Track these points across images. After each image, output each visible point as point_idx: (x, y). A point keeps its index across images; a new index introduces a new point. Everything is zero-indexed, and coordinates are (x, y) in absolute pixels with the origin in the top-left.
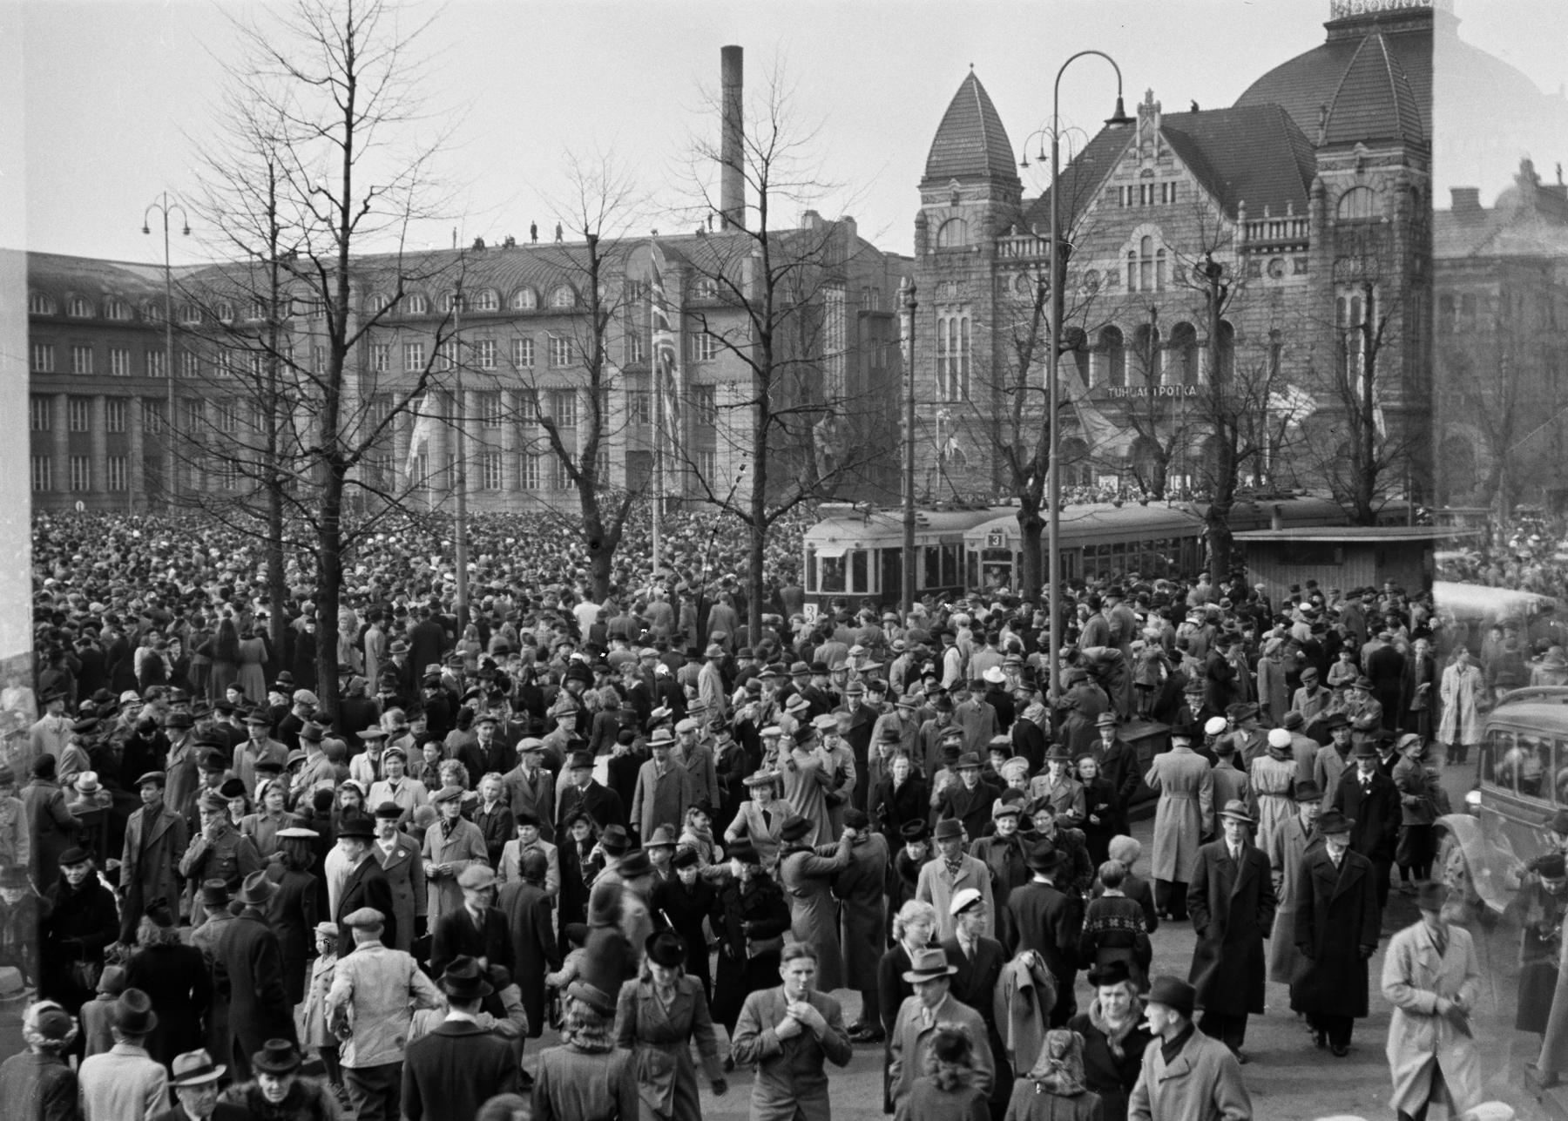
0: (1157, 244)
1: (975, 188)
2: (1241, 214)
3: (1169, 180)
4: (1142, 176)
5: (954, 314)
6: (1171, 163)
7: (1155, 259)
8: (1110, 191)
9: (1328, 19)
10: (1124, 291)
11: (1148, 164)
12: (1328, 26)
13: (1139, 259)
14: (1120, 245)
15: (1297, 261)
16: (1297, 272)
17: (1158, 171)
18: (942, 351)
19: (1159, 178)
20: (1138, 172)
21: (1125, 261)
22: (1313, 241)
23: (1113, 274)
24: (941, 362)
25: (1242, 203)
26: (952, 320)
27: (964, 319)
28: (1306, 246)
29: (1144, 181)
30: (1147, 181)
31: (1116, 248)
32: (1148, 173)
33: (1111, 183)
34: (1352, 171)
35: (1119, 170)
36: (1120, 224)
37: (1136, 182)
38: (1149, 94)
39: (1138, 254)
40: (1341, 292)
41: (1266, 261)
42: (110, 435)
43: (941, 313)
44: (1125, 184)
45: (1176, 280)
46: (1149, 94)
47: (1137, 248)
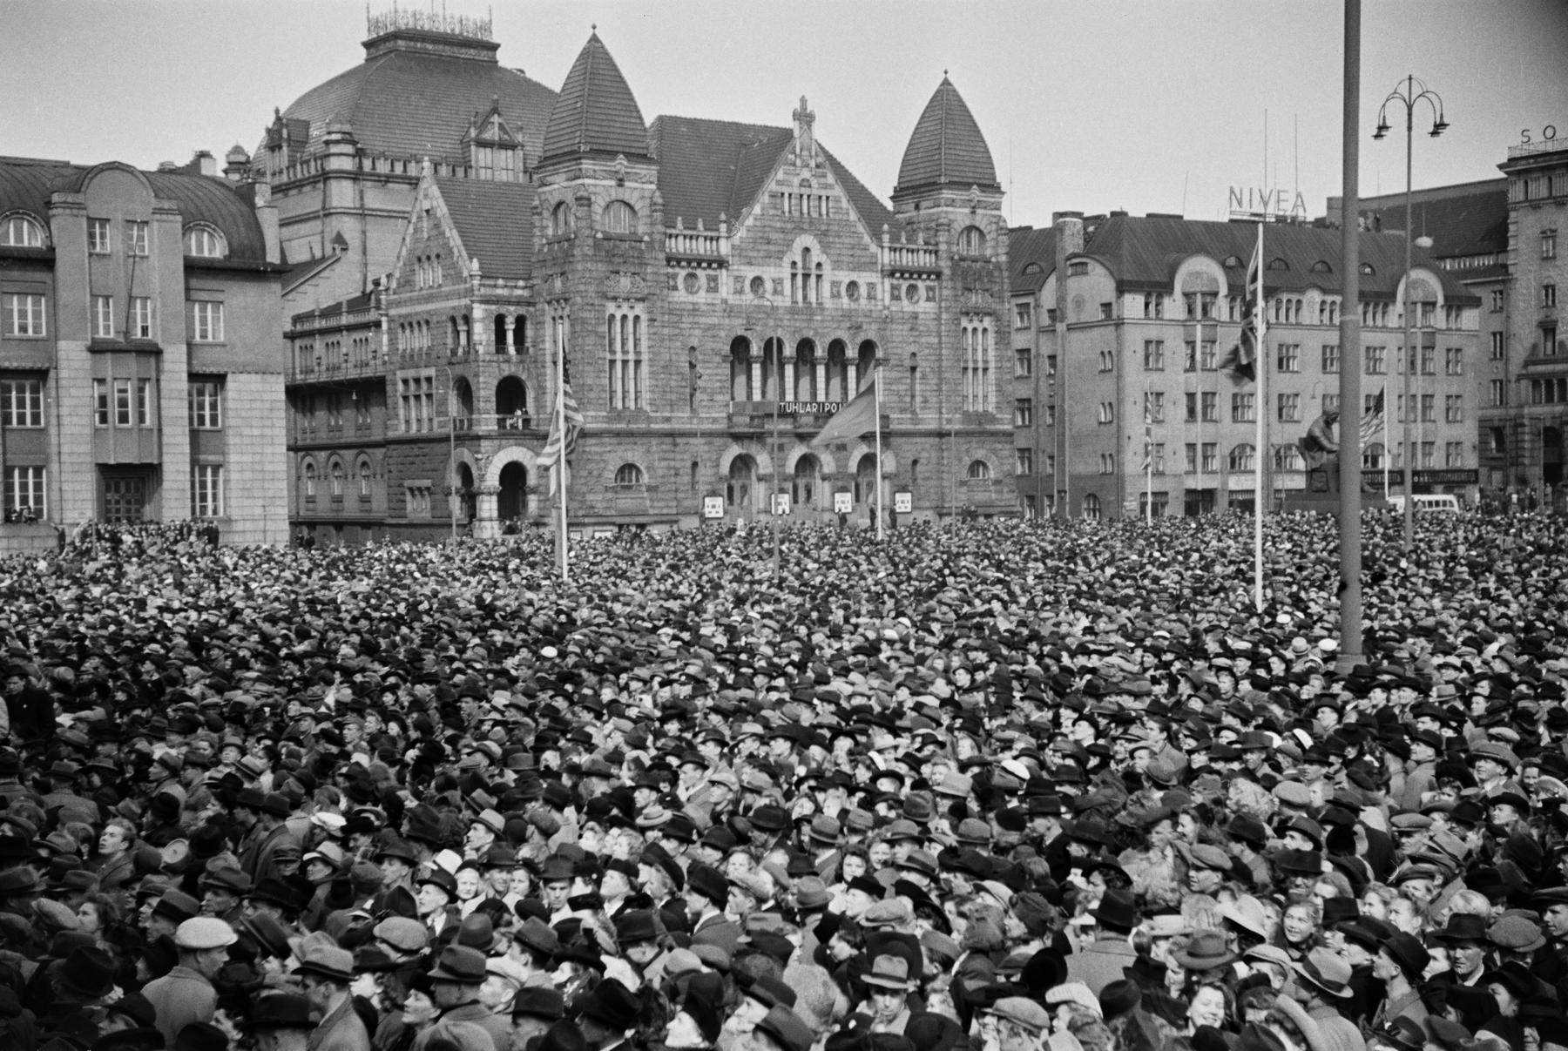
0: (816, 256)
1: (641, 169)
2: (886, 238)
3: (824, 193)
4: (801, 185)
5: (625, 310)
6: (824, 176)
7: (814, 272)
8: (773, 196)
9: (365, 38)
10: (788, 303)
11: (806, 174)
12: (368, 45)
13: (800, 271)
14: (783, 253)
15: (929, 289)
16: (928, 299)
17: (814, 182)
18: (613, 352)
19: (815, 192)
20: (796, 181)
21: (786, 272)
22: (947, 272)
23: (777, 282)
24: (612, 362)
25: (886, 227)
26: (624, 317)
27: (637, 318)
28: (939, 275)
29: (803, 191)
30: (805, 191)
31: (779, 256)
32: (805, 183)
33: (772, 186)
34: (967, 211)
35: (780, 175)
36: (783, 231)
37: (796, 191)
38: (803, 101)
39: (800, 265)
40: (964, 322)
41: (682, 273)
42: (24, 407)
43: (611, 308)
44: (786, 191)
45: (833, 296)
46: (803, 101)
47: (799, 259)
